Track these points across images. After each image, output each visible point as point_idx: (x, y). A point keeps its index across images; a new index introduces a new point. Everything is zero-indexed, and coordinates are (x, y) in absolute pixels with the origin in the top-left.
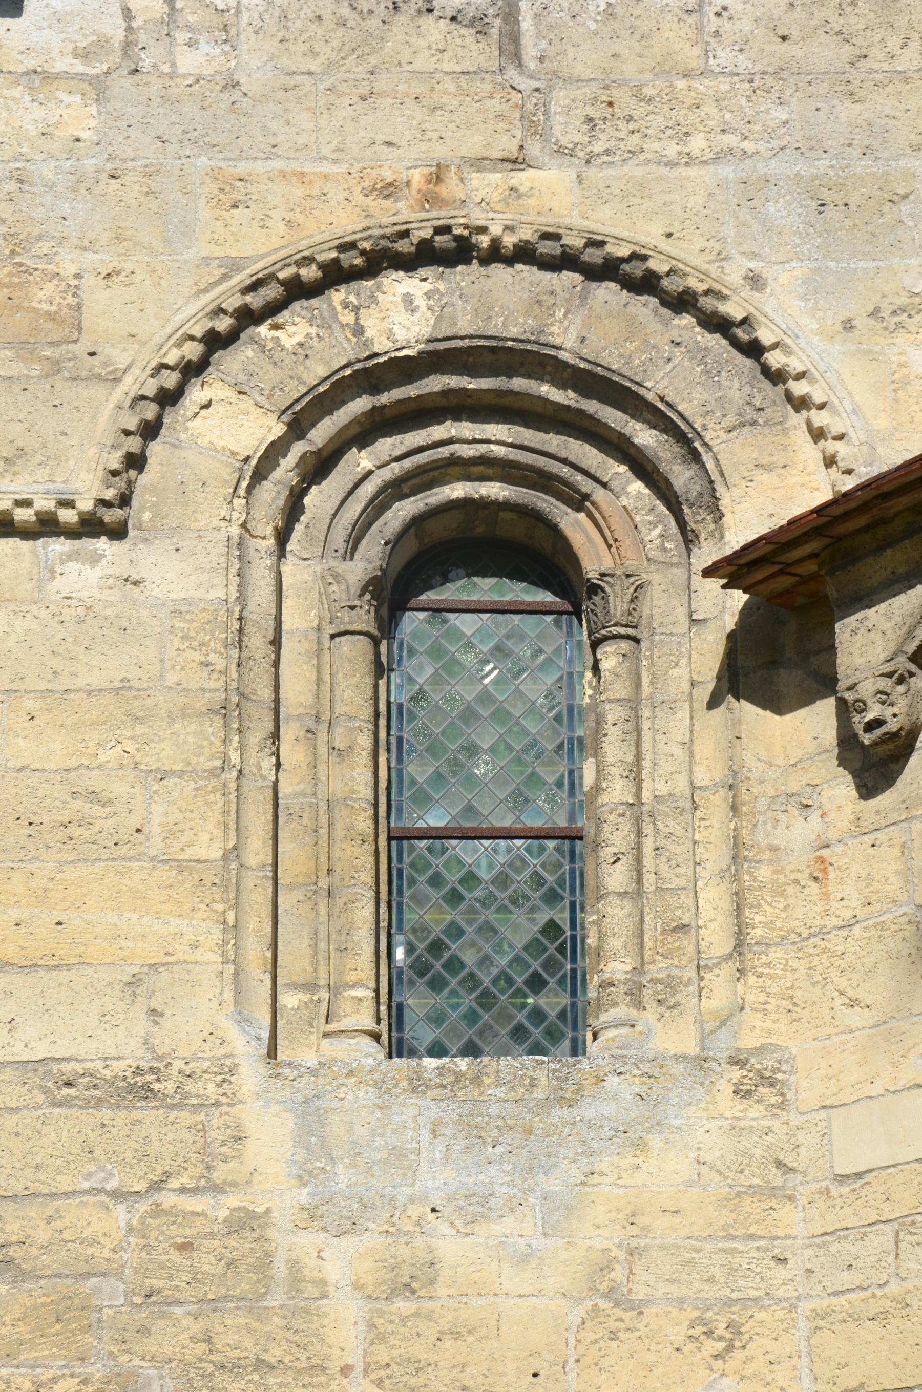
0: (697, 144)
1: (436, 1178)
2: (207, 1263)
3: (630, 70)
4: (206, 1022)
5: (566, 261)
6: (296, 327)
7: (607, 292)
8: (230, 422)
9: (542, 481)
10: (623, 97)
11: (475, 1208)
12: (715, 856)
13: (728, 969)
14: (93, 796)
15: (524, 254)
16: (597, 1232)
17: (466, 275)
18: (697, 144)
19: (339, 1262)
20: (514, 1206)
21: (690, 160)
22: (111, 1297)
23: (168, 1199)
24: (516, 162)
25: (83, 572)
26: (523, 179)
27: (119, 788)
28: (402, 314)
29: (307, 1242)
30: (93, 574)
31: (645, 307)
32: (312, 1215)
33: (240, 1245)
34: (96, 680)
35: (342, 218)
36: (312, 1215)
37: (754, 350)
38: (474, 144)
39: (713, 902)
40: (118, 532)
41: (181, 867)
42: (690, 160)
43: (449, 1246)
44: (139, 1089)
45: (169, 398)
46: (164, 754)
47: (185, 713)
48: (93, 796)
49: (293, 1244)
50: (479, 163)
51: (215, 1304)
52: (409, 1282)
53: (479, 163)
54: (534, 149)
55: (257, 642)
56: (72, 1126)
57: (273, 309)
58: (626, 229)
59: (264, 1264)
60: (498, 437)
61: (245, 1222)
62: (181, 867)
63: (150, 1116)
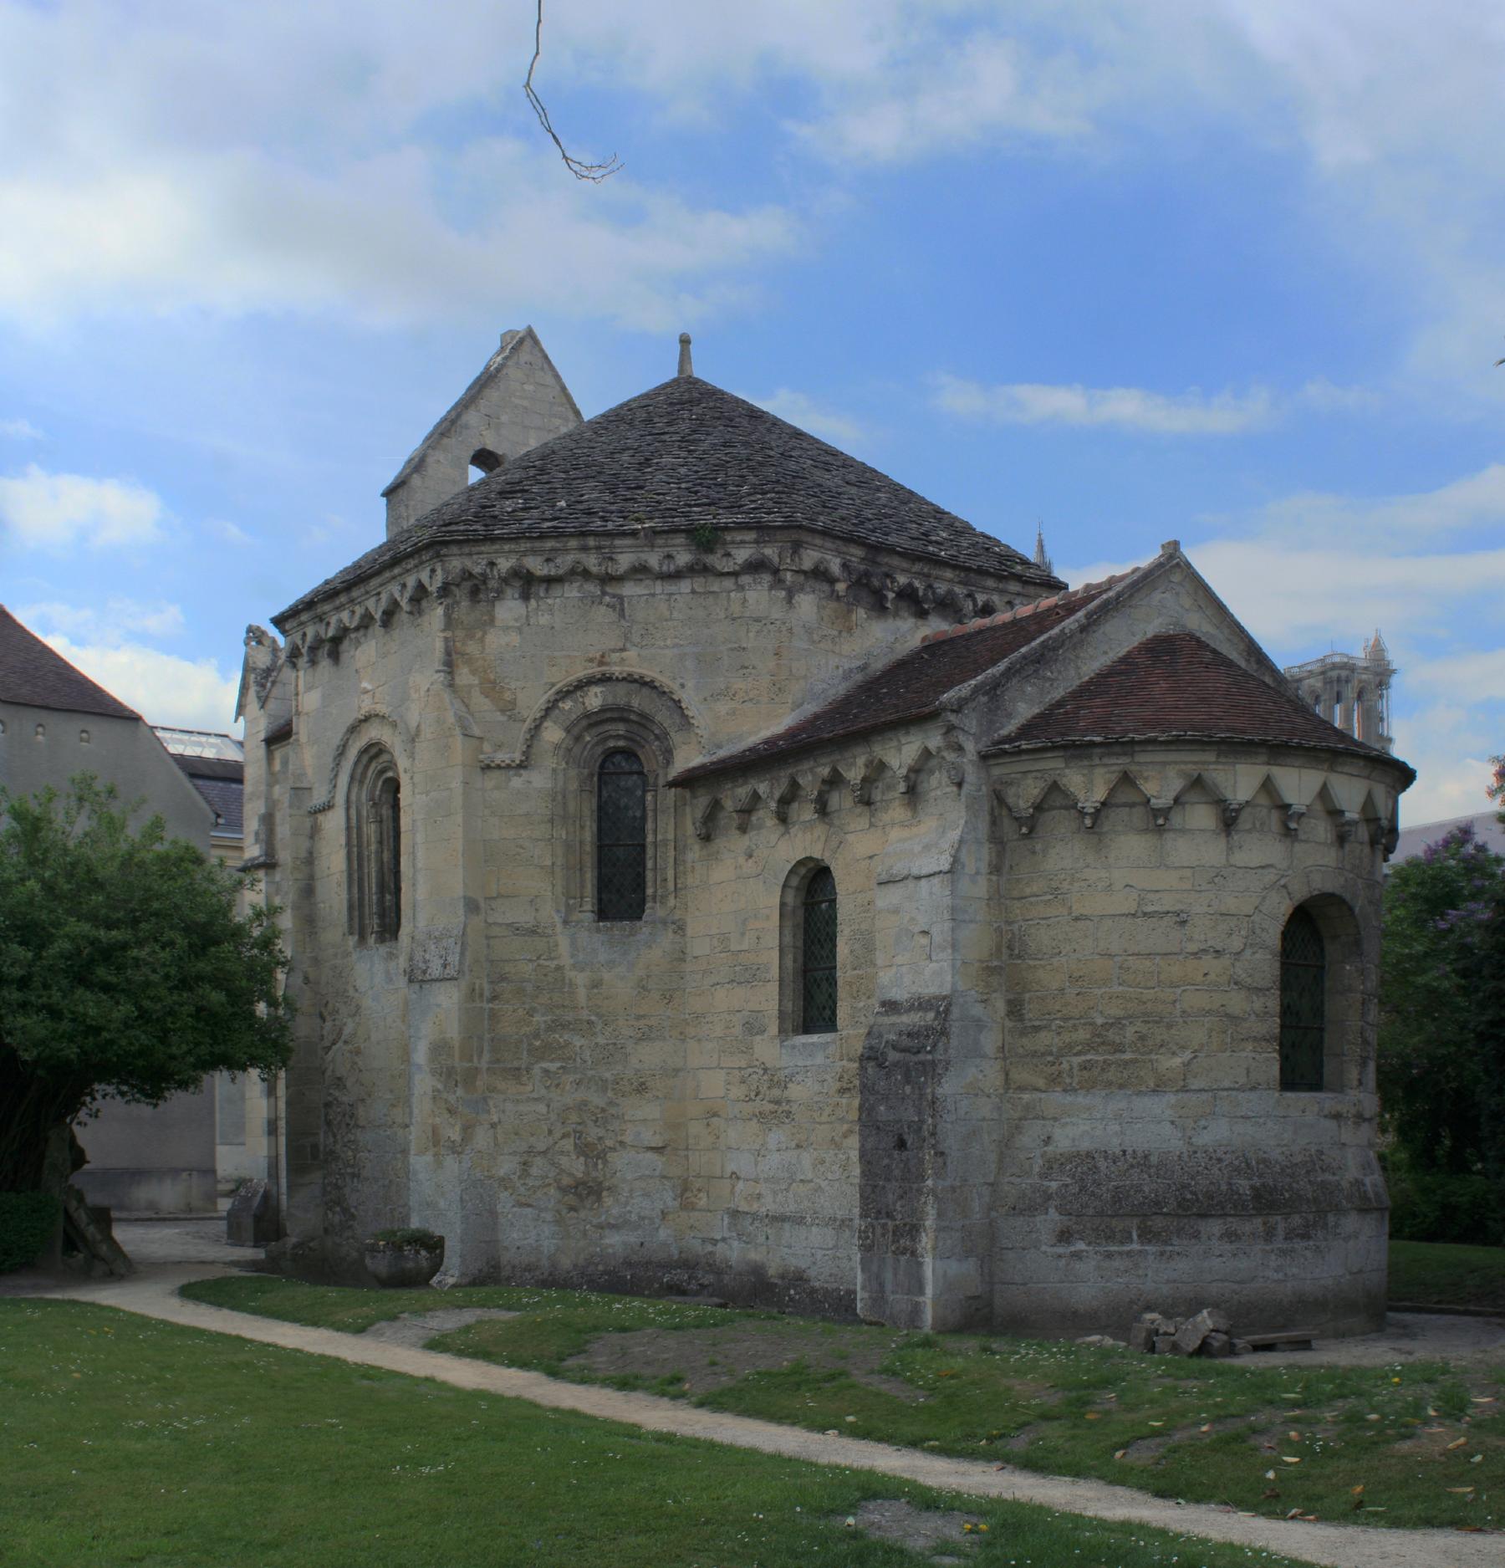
0: (669, 642)
4: (550, 913)
5: (635, 681)
6: (567, 705)
7: (645, 691)
8: (553, 734)
9: (631, 740)
10: (650, 627)
12: (671, 860)
15: (624, 679)
18: (669, 642)
19: (581, 979)
21: (667, 647)
22: (529, 988)
24: (623, 650)
25: (517, 782)
26: (624, 654)
28: (594, 699)
29: (573, 974)
35: (581, 673)
36: (574, 966)
39: (670, 874)
40: (525, 767)
42: (667, 647)
43: (606, 976)
44: (533, 932)
45: (538, 727)
49: (571, 974)
50: (613, 651)
52: (596, 985)
53: (613, 651)
54: (628, 645)
55: (560, 797)
57: (562, 699)
58: (649, 673)
60: (621, 729)
61: (559, 968)
62: (542, 867)
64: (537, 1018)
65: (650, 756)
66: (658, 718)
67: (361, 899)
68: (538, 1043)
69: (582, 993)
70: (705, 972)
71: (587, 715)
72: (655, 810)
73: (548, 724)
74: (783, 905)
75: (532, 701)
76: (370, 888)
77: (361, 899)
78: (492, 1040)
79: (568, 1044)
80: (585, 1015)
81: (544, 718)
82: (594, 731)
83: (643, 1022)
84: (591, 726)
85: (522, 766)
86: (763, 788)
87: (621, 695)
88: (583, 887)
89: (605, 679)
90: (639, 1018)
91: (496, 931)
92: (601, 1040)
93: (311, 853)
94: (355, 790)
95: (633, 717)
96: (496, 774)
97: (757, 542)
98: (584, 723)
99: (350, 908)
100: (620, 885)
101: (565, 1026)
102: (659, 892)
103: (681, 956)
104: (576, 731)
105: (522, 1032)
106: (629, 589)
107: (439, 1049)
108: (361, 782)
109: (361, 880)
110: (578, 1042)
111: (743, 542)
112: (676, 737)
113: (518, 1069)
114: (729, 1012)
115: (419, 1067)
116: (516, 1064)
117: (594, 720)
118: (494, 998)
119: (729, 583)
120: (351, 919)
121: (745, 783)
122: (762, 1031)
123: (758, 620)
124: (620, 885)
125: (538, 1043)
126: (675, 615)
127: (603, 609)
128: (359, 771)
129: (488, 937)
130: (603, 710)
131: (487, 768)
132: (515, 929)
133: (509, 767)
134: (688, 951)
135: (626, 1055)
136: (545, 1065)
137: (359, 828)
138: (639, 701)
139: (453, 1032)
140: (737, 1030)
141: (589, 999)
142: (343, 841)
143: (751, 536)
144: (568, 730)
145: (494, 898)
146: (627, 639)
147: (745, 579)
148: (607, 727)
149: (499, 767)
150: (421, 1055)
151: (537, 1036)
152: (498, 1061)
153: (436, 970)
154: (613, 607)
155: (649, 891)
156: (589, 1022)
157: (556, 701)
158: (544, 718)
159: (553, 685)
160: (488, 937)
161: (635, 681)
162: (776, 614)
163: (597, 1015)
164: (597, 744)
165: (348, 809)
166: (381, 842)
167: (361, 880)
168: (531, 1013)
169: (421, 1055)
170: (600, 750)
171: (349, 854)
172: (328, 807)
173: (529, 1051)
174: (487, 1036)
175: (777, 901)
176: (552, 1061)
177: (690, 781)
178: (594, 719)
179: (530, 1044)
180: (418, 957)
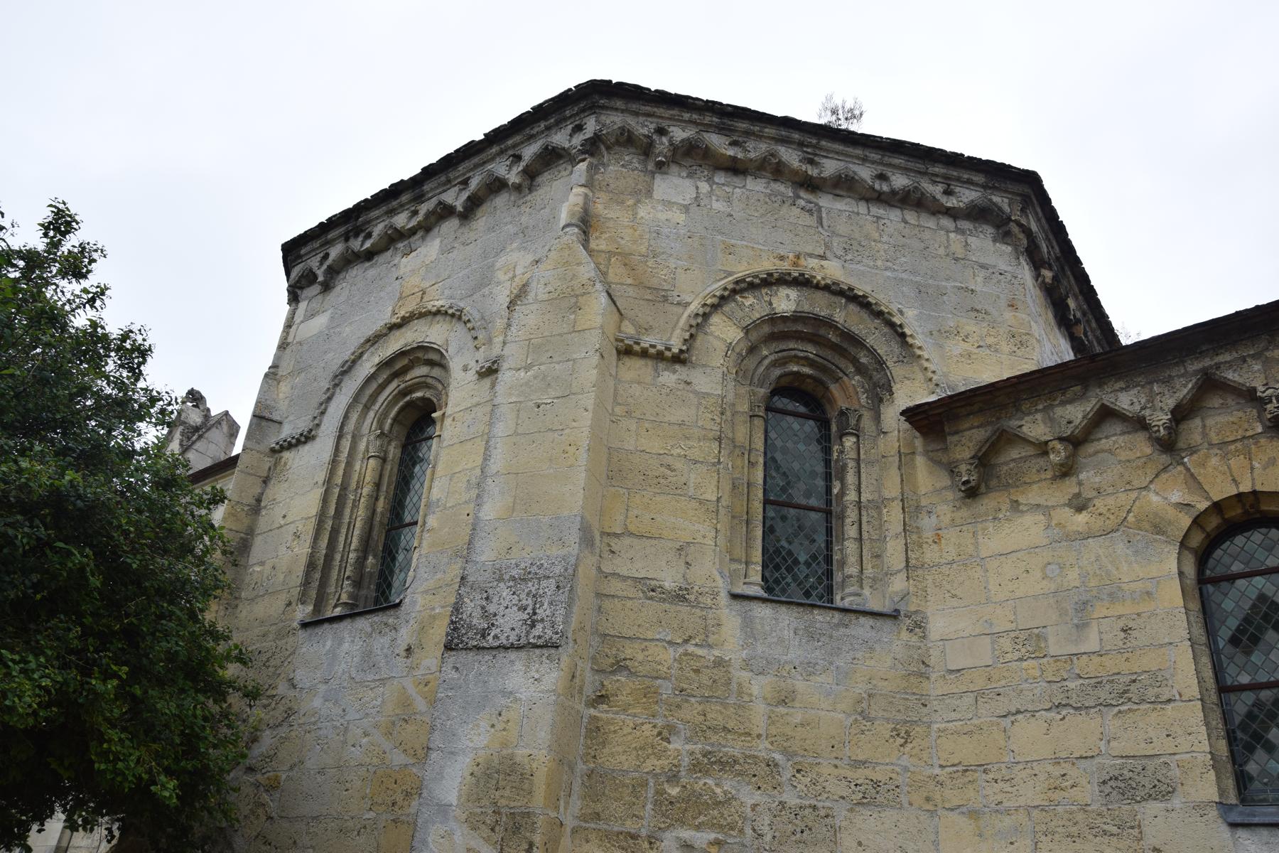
0: (879, 263)
1: (796, 652)
2: (705, 679)
3: (857, 235)
4: (710, 572)
5: (841, 293)
6: (749, 300)
7: (853, 307)
9: (823, 369)
11: (810, 669)
13: (903, 575)
14: (669, 467)
15: (827, 288)
16: (861, 688)
17: (806, 292)
18: (879, 263)
19: (759, 686)
20: (825, 670)
22: (666, 689)
23: (691, 649)
24: (823, 257)
25: (669, 377)
26: (823, 263)
27: (678, 465)
28: (786, 301)
29: (745, 675)
30: (674, 377)
31: (864, 315)
32: (747, 665)
33: (718, 674)
34: (673, 419)
35: (767, 265)
36: (747, 665)
37: (903, 335)
38: (809, 249)
41: (701, 502)
42: (877, 268)
43: (800, 685)
44: (680, 597)
45: (706, 316)
46: (695, 454)
47: (705, 438)
48: (669, 467)
50: (811, 255)
51: (707, 699)
52: (785, 699)
53: (811, 255)
54: (828, 254)
56: (653, 609)
57: (741, 291)
58: (862, 288)
59: (728, 683)
60: (811, 350)
61: (719, 663)
62: (701, 502)
63: (684, 609)
64: (676, 745)
65: (848, 392)
66: (870, 341)
67: (329, 558)
68: (674, 791)
69: (758, 715)
70: (979, 694)
71: (773, 319)
72: (858, 461)
73: (716, 319)
74: (1181, 574)
75: (696, 290)
76: (347, 543)
77: (329, 558)
78: (590, 774)
79: (729, 800)
80: (762, 748)
81: (715, 307)
82: (775, 346)
83: (860, 775)
84: (772, 337)
85: (679, 359)
86: (1127, 401)
87: (820, 305)
88: (748, 547)
89: (802, 282)
90: (857, 764)
91: (615, 587)
92: (792, 800)
93: (259, 500)
94: (354, 417)
95: (832, 336)
96: (637, 363)
97: (985, 187)
98: (766, 329)
99: (311, 566)
100: (799, 559)
101: (727, 765)
102: (869, 571)
103: (921, 669)
104: (754, 336)
105: (648, 766)
106: (825, 201)
107: (500, 774)
108: (367, 408)
109: (335, 532)
110: (748, 796)
111: (969, 182)
112: (897, 371)
113: (634, 837)
114: (1056, 761)
115: (443, 809)
116: (630, 826)
117: (779, 330)
118: (601, 699)
119: (947, 222)
120: (306, 583)
121: (1081, 397)
122: (1163, 792)
123: (983, 266)
124: (799, 559)
125: (674, 791)
126: (885, 238)
127: (796, 211)
128: (369, 391)
129: (599, 595)
130: (797, 317)
131: (626, 352)
132: (652, 590)
133: (660, 356)
134: (932, 661)
135: (835, 830)
136: (686, 834)
137: (349, 464)
138: (845, 316)
139: (536, 750)
140: (1088, 792)
141: (771, 721)
142: (321, 476)
143: (979, 178)
144: (747, 330)
145: (616, 535)
146: (827, 246)
147: (965, 225)
148: (792, 345)
149: (644, 354)
150: (451, 783)
151: (673, 778)
152: (597, 816)
153: (509, 623)
154: (810, 211)
155: (852, 570)
156: (772, 765)
157: (734, 292)
158: (715, 307)
159: (730, 274)
160: (599, 595)
161: (841, 293)
162: (1003, 266)
163: (785, 752)
164: (774, 364)
165: (340, 437)
166: (378, 485)
167: (335, 532)
168: (666, 733)
169: (451, 783)
170: (777, 372)
171: (327, 493)
172: (306, 438)
173: (655, 803)
174: (581, 767)
175: (1175, 570)
176: (698, 828)
177: (931, 421)
178: (781, 327)
179: (661, 792)
180: (471, 607)
